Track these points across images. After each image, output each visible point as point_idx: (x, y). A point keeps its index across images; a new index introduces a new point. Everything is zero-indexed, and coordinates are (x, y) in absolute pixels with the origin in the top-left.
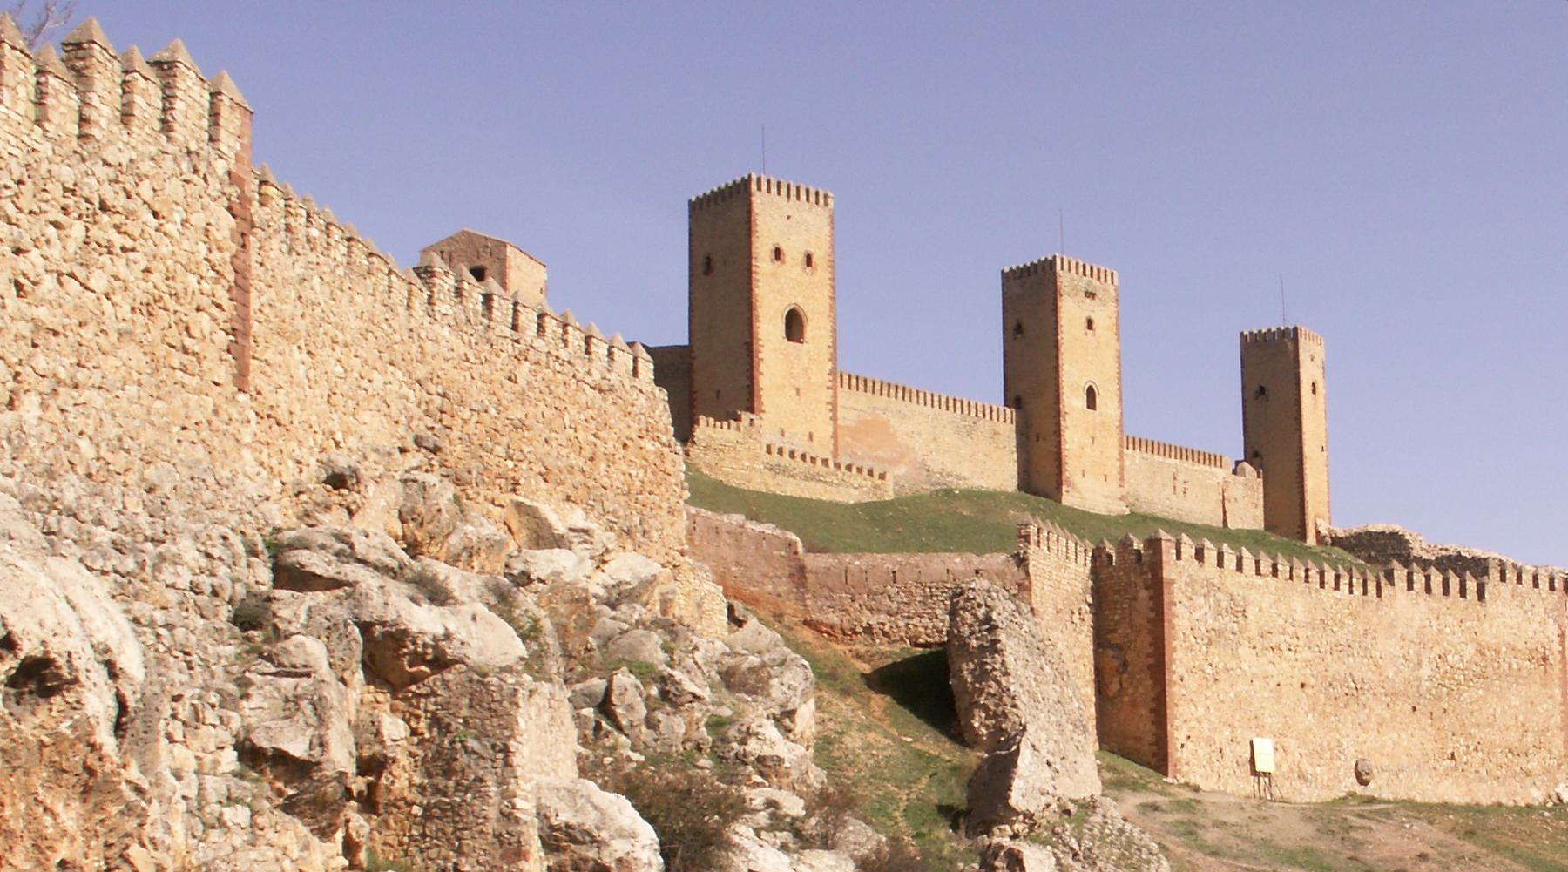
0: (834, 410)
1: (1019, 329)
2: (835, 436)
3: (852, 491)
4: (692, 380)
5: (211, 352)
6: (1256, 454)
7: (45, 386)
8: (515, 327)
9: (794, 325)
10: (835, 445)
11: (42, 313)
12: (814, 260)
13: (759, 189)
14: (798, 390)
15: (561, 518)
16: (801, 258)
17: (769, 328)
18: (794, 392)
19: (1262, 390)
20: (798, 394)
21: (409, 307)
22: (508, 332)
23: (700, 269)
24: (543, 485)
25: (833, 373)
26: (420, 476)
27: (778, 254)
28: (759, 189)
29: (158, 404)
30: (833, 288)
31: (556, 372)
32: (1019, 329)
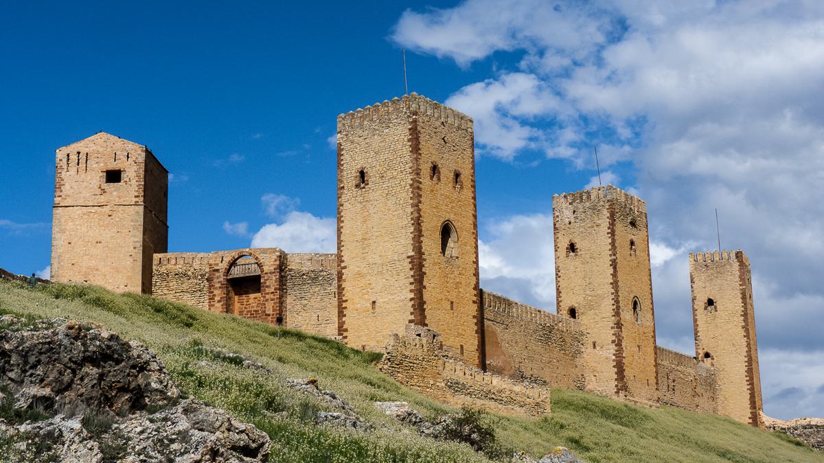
1: (572, 248)
3: (518, 409)
4: (340, 289)
6: (707, 355)
14: (452, 303)
16: (452, 175)
18: (449, 306)
19: (710, 302)
20: (452, 309)
27: (435, 169)
30: (475, 206)
32: (572, 248)
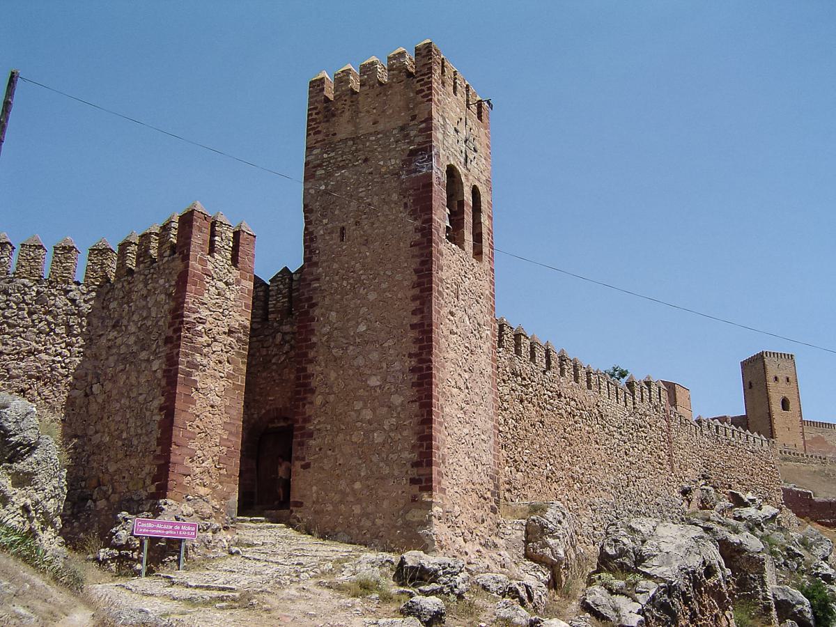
0: (803, 435)
2: (804, 445)
5: (665, 462)
7: (634, 479)
8: (726, 435)
9: (785, 404)
10: (805, 447)
11: (631, 459)
12: (790, 379)
13: (767, 356)
15: (748, 496)
16: (785, 380)
17: (776, 407)
21: (696, 434)
22: (724, 437)
23: (748, 386)
24: (739, 486)
25: (801, 420)
26: (706, 487)
27: (776, 378)
28: (767, 356)
29: (656, 480)
31: (739, 448)
